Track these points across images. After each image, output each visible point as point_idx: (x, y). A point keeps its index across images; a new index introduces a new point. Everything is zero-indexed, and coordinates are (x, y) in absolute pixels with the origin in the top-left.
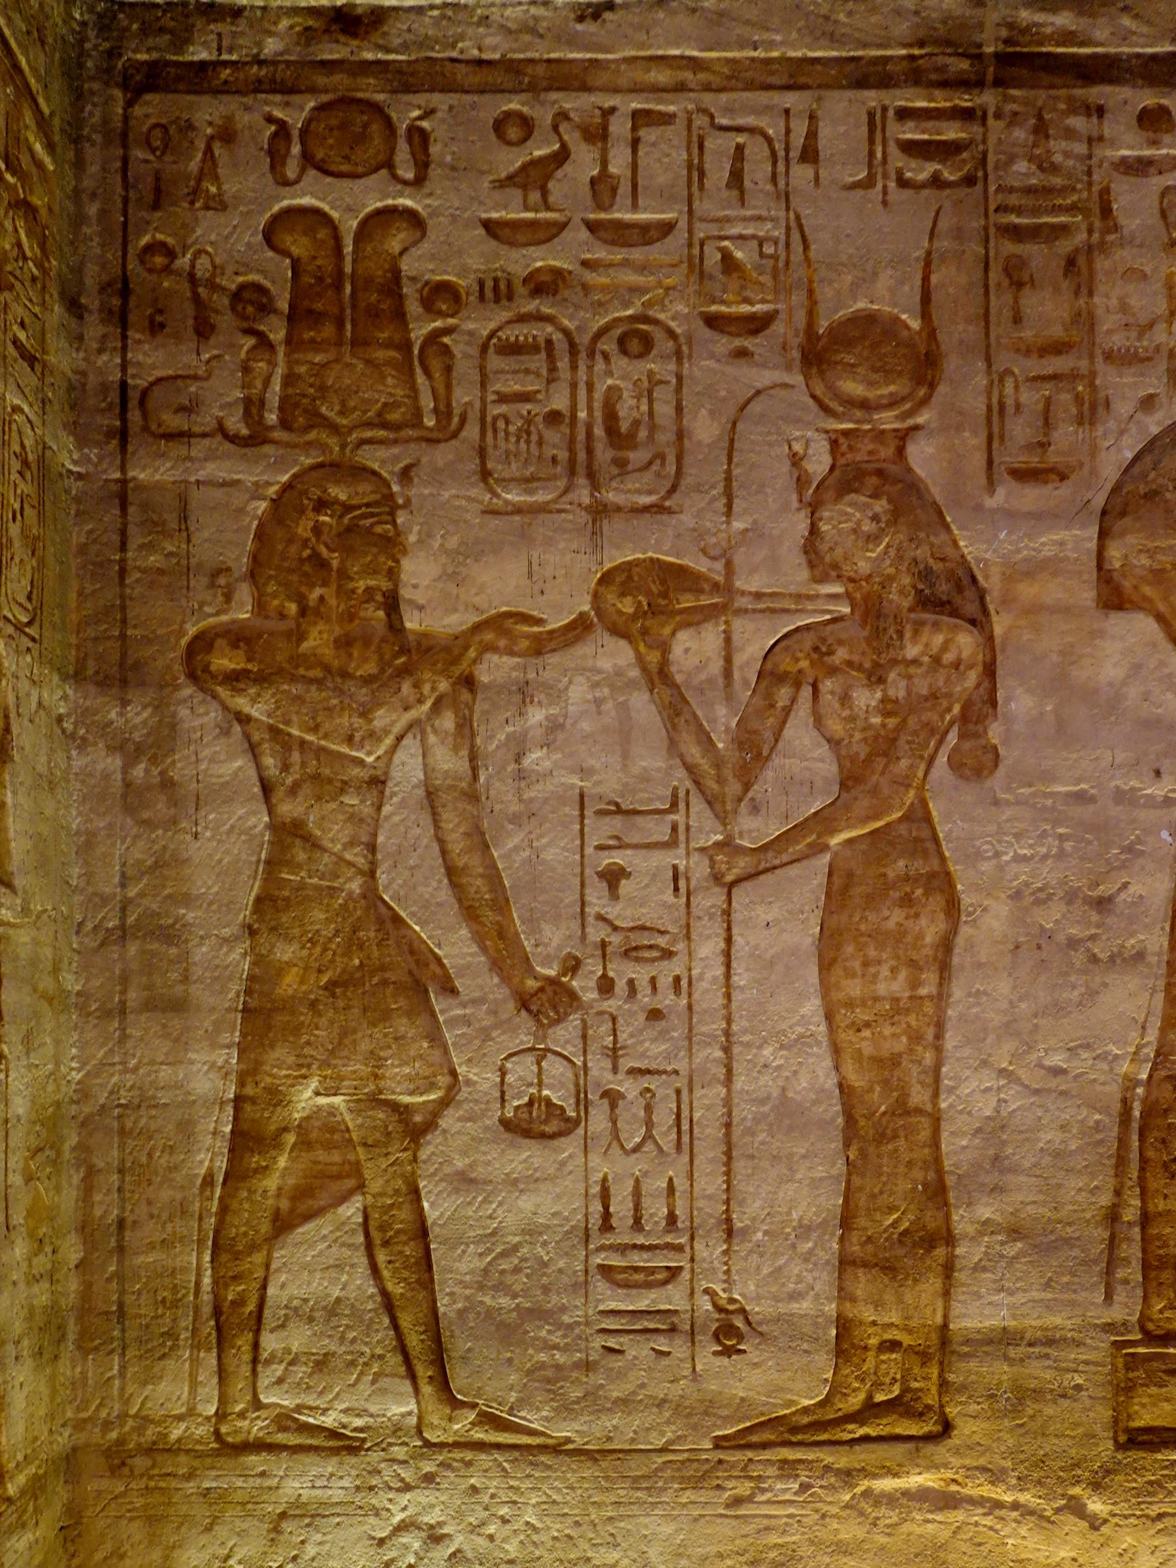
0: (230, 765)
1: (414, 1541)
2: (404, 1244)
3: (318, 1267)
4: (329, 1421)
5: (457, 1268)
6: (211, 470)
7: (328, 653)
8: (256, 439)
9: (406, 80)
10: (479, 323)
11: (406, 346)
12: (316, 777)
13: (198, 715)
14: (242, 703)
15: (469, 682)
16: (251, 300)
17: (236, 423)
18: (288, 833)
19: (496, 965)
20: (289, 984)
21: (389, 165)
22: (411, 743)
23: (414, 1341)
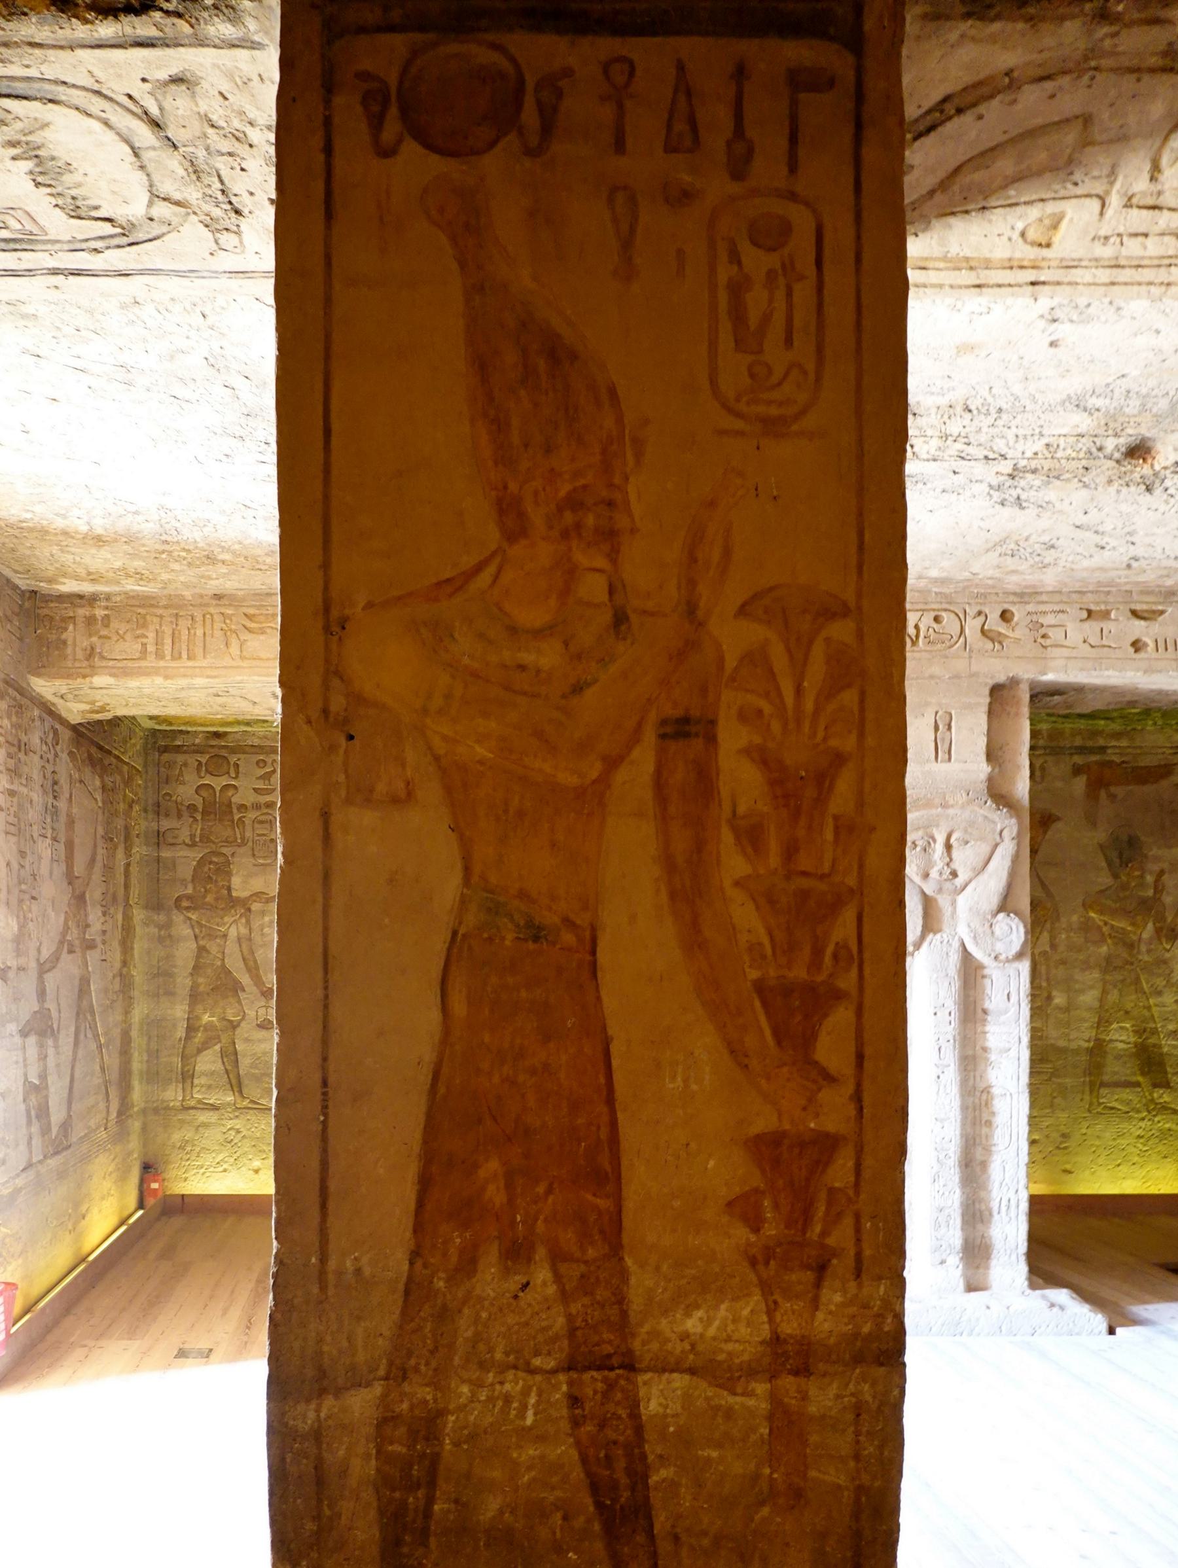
0: (187, 931)
1: (233, 1133)
2: (231, 1056)
3: (208, 1062)
4: (211, 1102)
5: (245, 1063)
6: (181, 854)
7: (212, 902)
8: (193, 845)
9: (233, 750)
10: (252, 815)
11: (233, 821)
12: (209, 935)
13: (177, 918)
14: (189, 915)
15: (249, 910)
16: (192, 808)
17: (188, 841)
18: (202, 950)
19: (256, 985)
20: (201, 988)
21: (228, 773)
22: (234, 926)
23: (234, 1081)
